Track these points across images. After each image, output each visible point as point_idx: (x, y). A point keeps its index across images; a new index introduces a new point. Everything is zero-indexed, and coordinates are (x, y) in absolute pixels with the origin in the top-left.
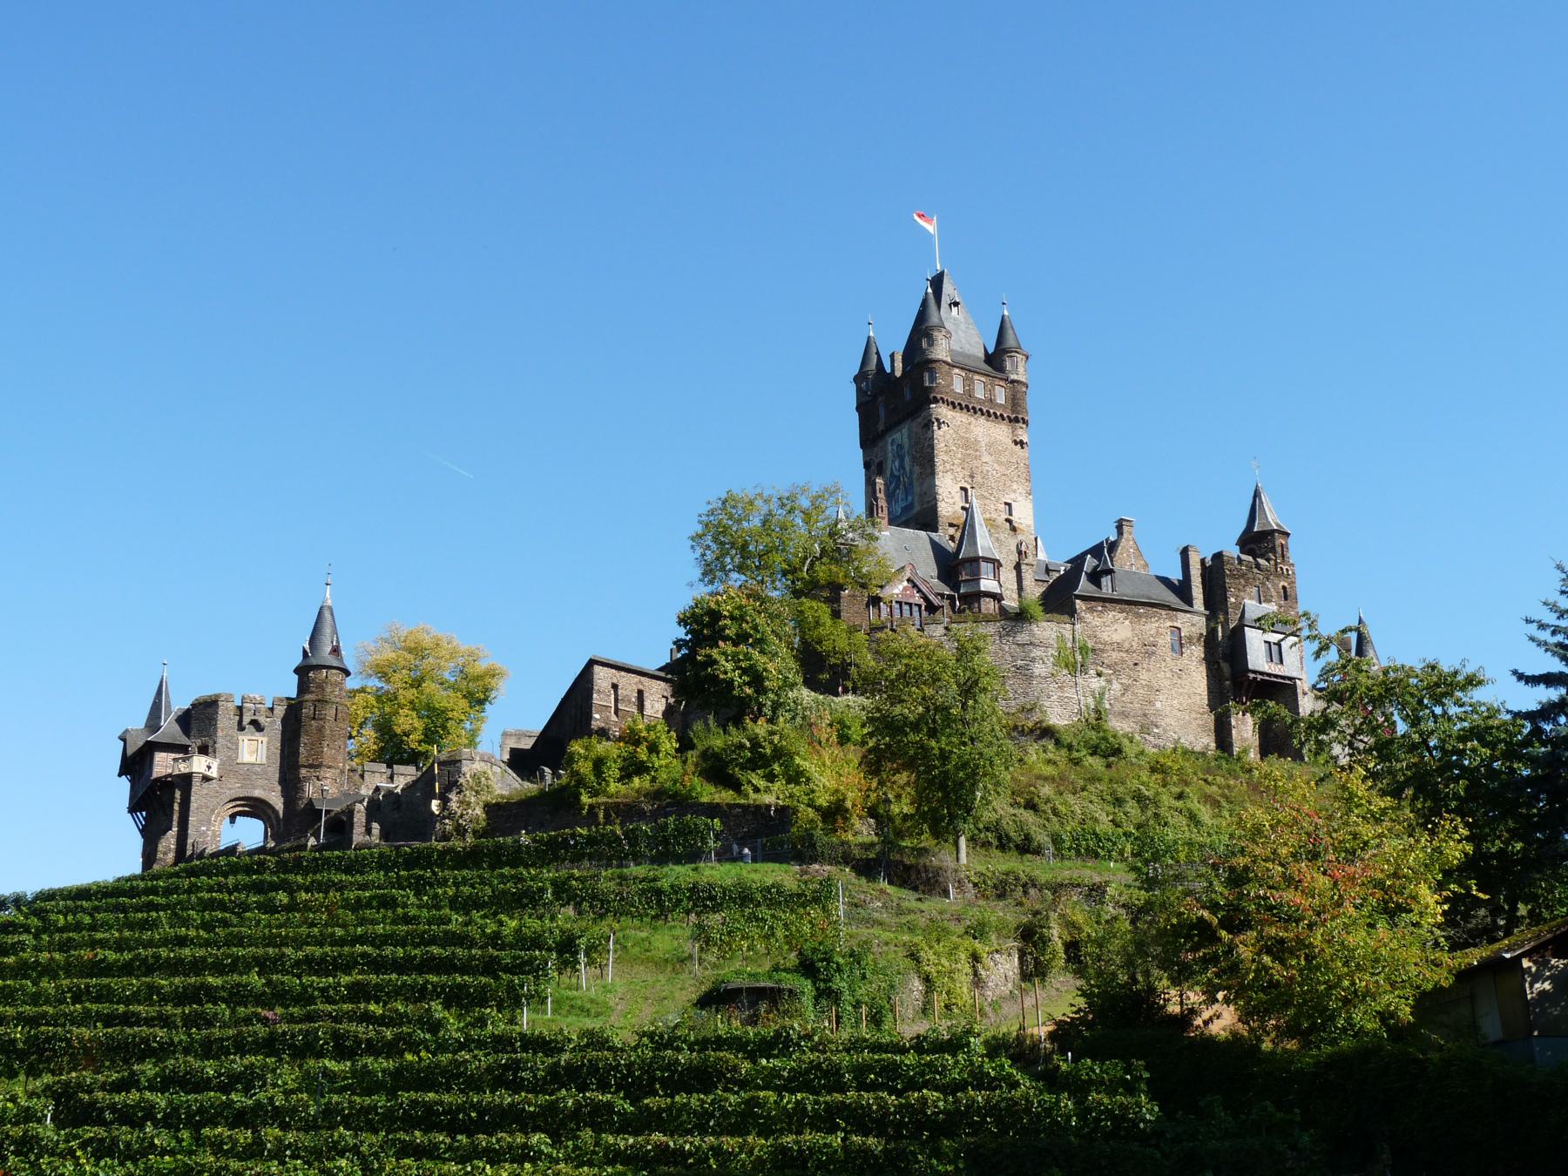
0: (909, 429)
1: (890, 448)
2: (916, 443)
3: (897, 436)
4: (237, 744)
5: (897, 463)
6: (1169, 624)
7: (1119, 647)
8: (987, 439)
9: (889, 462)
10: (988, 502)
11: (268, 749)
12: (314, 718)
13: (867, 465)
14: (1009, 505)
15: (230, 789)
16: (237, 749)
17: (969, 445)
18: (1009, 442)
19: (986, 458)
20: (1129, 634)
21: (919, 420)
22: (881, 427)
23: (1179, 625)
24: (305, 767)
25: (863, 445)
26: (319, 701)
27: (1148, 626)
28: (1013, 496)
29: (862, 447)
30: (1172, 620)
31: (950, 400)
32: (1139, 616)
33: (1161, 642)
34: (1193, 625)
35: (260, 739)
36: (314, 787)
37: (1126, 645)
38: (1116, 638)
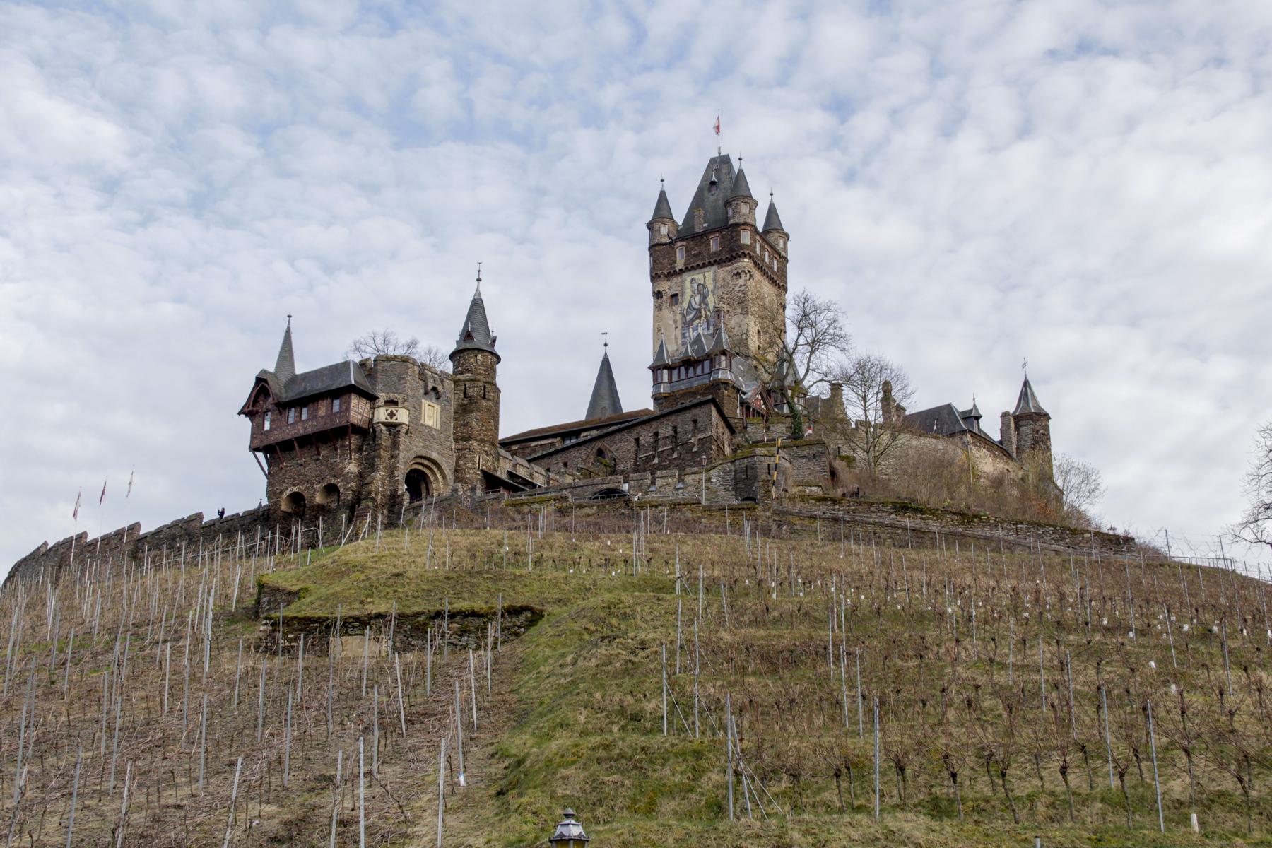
0: (715, 273)
1: (688, 285)
2: (723, 286)
3: (698, 276)
4: (420, 406)
5: (698, 299)
9: (687, 297)
11: (441, 418)
12: (484, 398)
13: (658, 295)
15: (417, 447)
16: (420, 411)
21: (729, 268)
22: (680, 264)
24: (477, 440)
25: (654, 278)
26: (488, 383)
29: (652, 281)
35: (436, 406)
36: (483, 460)
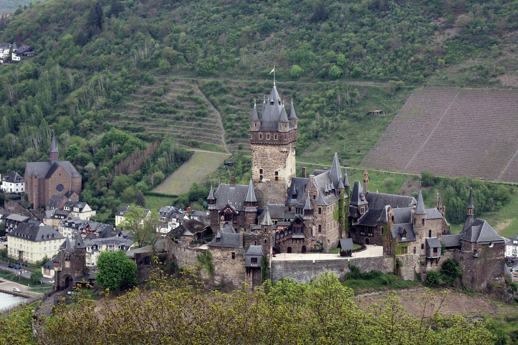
6: (231, 252)
7: (217, 258)
8: (270, 153)
10: (269, 173)
14: (277, 173)
17: (264, 156)
18: (278, 151)
19: (270, 159)
20: (220, 255)
23: (234, 251)
27: (225, 253)
28: (279, 169)
30: (232, 250)
31: (257, 142)
32: (222, 250)
33: (228, 256)
34: (239, 251)
37: (219, 258)
38: (217, 256)
